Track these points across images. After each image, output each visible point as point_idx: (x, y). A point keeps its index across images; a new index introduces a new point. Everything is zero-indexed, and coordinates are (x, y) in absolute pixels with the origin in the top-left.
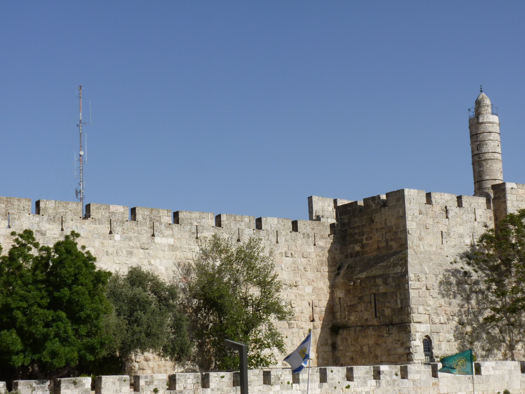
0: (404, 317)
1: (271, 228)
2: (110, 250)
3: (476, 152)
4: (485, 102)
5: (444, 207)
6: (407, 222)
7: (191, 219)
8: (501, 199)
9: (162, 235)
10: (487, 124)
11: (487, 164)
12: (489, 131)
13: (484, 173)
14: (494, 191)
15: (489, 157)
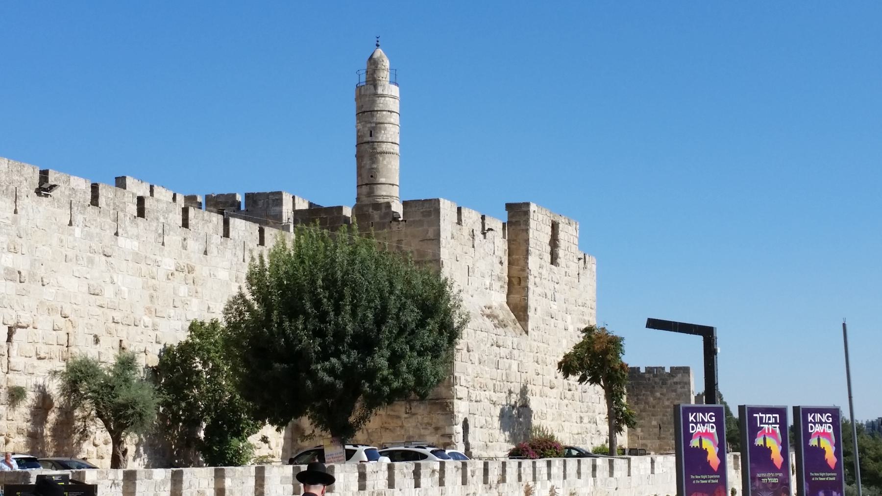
0: (439, 390)
1: (239, 237)
2: (71, 254)
3: (369, 139)
4: (384, 64)
5: (471, 231)
6: (441, 249)
7: (158, 211)
8: (520, 225)
9: (126, 235)
10: (387, 99)
11: (384, 159)
12: (390, 110)
13: (378, 172)
14: (509, 213)
15: (388, 149)
